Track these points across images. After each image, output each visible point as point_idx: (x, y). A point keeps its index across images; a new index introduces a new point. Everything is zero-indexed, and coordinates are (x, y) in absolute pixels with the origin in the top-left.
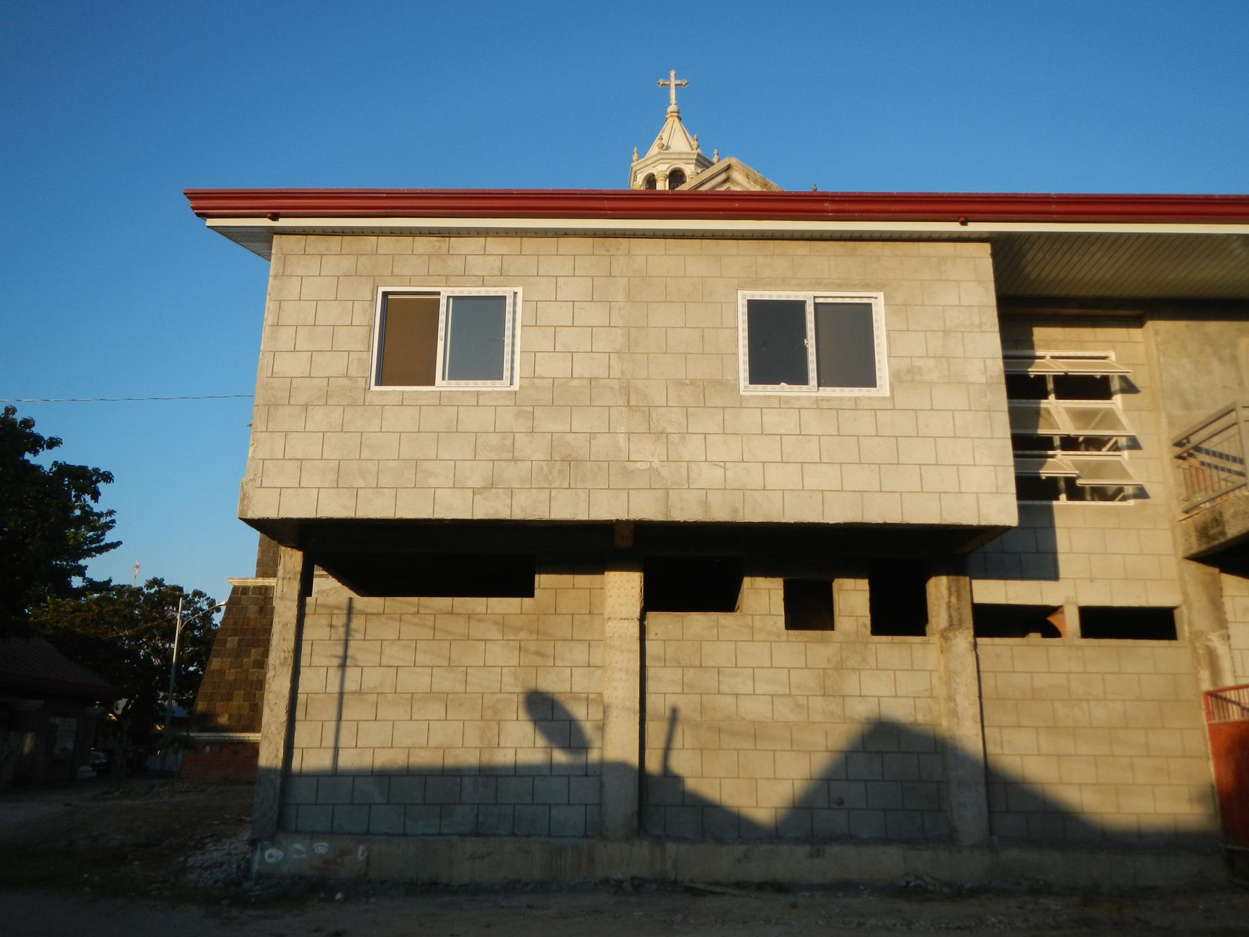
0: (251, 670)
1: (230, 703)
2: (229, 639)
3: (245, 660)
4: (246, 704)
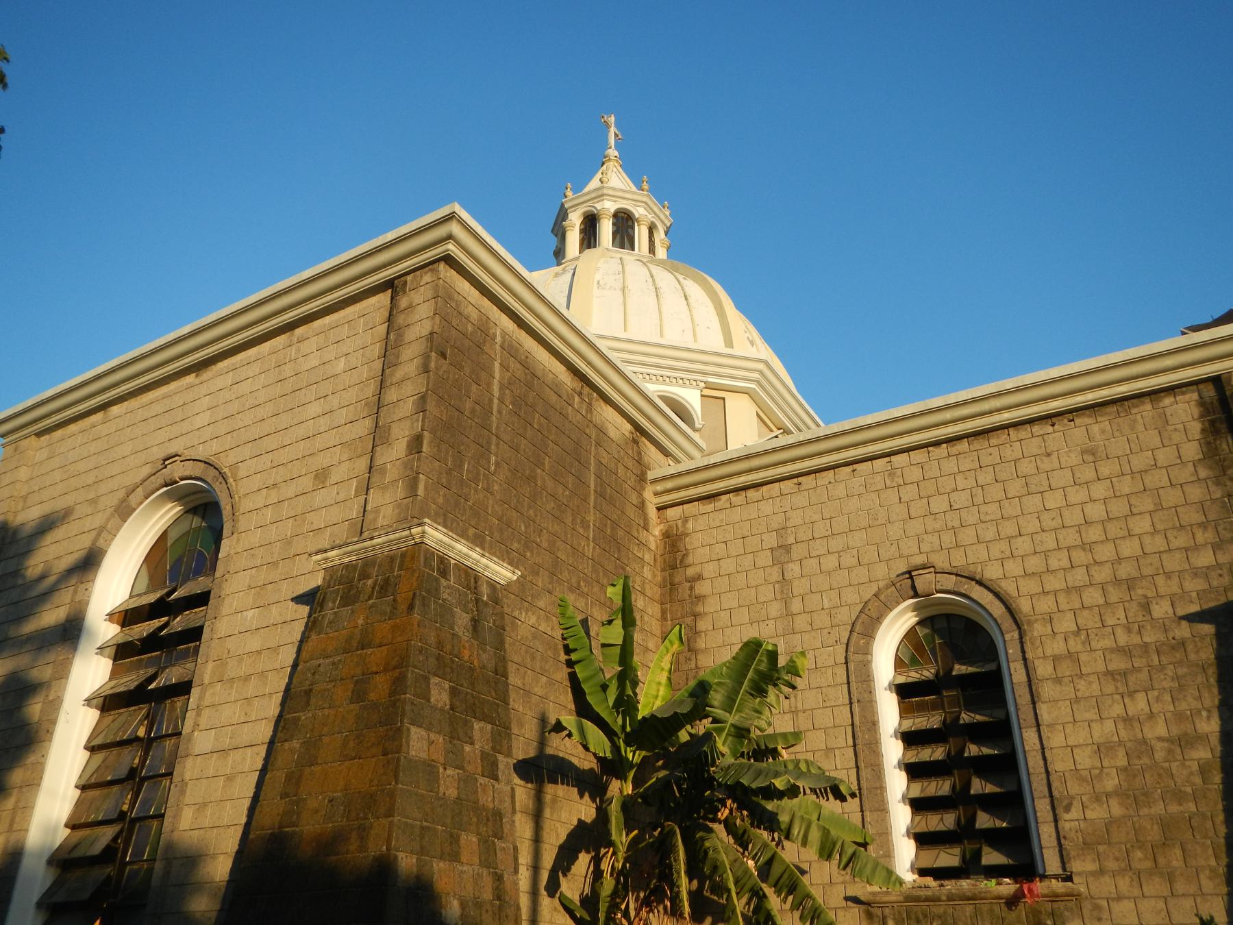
0: (481, 780)
1: (460, 868)
2: (434, 680)
3: (467, 748)
4: (485, 872)
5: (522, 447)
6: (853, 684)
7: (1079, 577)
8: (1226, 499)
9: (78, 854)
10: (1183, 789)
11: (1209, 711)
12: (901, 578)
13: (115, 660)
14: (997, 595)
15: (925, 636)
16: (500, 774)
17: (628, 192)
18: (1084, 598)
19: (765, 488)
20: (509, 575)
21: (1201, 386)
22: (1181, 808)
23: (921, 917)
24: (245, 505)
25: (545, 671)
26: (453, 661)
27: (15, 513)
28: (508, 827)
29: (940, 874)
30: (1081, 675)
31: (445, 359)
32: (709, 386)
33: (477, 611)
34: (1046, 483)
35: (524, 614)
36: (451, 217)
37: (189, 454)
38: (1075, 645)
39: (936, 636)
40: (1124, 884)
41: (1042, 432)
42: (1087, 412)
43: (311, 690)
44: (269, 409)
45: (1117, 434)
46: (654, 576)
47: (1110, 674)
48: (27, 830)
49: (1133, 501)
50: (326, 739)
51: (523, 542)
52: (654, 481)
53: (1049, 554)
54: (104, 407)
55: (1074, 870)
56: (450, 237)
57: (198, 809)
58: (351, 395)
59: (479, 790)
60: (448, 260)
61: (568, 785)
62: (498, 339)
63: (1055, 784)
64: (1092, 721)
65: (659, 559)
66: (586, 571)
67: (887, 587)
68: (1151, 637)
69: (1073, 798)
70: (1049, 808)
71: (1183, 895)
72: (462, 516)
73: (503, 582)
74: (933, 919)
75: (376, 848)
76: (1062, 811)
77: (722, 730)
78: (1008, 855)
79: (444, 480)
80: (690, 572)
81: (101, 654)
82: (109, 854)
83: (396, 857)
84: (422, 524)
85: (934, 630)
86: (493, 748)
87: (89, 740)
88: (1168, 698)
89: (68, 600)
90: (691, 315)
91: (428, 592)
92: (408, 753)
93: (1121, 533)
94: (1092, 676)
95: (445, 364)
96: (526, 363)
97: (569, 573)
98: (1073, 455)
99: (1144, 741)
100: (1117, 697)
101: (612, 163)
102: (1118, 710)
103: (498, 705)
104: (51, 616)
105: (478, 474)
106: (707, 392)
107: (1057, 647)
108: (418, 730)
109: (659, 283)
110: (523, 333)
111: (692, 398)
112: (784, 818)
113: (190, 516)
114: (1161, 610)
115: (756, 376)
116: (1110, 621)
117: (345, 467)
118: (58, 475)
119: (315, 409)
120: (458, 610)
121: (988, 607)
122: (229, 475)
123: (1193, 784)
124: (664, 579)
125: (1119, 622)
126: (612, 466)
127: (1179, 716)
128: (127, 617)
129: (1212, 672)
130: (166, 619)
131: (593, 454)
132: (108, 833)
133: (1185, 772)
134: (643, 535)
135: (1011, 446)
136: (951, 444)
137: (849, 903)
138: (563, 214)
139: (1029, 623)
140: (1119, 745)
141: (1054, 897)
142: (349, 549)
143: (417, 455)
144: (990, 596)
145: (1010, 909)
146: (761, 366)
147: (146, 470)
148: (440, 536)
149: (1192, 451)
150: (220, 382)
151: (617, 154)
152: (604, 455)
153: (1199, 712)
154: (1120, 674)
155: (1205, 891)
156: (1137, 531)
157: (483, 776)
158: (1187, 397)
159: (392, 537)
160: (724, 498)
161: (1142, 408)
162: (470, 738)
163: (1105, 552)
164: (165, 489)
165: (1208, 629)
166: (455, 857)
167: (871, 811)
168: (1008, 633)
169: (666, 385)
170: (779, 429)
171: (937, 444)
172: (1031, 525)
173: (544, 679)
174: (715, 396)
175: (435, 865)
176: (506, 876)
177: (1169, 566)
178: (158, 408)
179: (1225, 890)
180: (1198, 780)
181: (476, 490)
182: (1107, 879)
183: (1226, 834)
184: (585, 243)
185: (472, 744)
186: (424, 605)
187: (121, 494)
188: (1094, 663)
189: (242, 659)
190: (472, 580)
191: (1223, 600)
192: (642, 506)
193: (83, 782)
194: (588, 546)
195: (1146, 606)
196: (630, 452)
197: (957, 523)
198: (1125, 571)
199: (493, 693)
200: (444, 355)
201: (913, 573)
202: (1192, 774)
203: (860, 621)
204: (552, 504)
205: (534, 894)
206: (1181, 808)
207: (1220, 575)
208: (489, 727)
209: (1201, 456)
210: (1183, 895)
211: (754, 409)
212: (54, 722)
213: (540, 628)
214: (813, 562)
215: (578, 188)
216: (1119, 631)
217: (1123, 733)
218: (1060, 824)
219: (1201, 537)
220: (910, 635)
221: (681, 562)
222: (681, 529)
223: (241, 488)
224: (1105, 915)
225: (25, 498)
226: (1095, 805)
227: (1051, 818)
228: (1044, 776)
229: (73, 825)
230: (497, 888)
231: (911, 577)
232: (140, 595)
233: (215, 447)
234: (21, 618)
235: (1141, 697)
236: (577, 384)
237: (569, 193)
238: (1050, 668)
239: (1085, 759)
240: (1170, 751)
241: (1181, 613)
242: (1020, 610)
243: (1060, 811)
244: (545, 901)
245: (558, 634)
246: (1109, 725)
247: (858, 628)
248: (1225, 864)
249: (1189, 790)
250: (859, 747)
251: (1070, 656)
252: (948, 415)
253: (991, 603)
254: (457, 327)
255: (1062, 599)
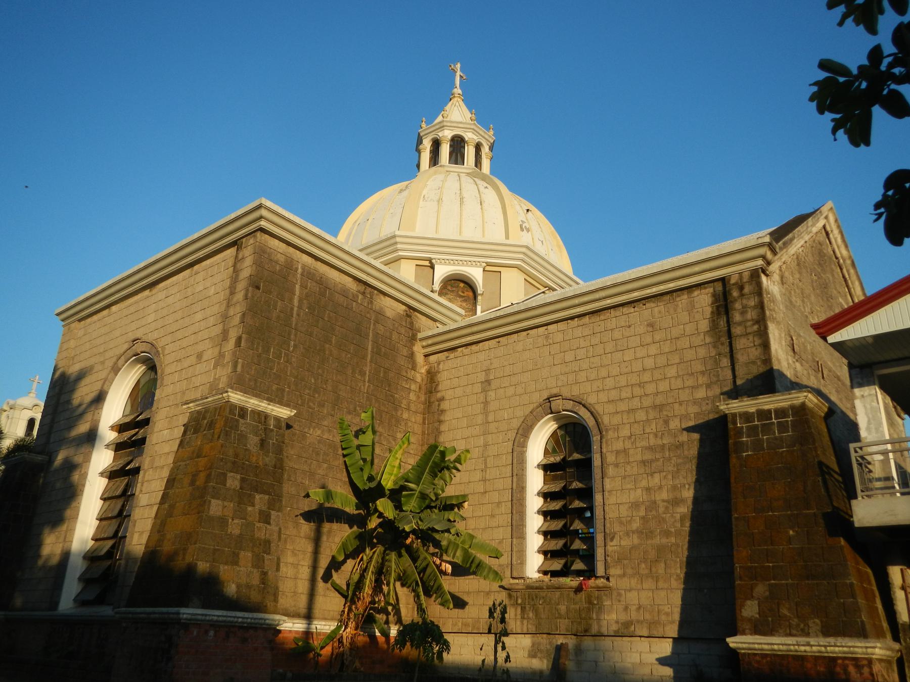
0: (258, 525)
1: (238, 569)
2: (230, 475)
3: (250, 509)
4: (255, 571)
5: (315, 333)
6: (515, 465)
7: (635, 404)
8: (717, 357)
9: (95, 554)
10: (670, 529)
11: (689, 485)
12: (545, 402)
13: (116, 451)
14: (592, 413)
15: (562, 436)
16: (271, 522)
17: (461, 123)
18: (636, 416)
19: (481, 344)
20: (289, 413)
21: (716, 284)
22: (668, 540)
23: (534, 597)
24: (168, 370)
25: (327, 461)
26: (244, 464)
27: (69, 367)
28: (275, 548)
29: (554, 574)
30: (628, 463)
31: (259, 289)
32: (488, 264)
33: (265, 435)
34: (626, 345)
35: (312, 430)
36: (260, 207)
37: (145, 338)
38: (628, 445)
39: (567, 436)
40: (634, 582)
41: (627, 312)
42: (653, 299)
43: (175, 478)
44: (179, 315)
45: (667, 314)
46: (418, 397)
47: (644, 462)
48: (72, 542)
49: (669, 357)
50: (178, 504)
51: (312, 389)
52: (421, 340)
53: (621, 388)
54: (108, 306)
55: (611, 574)
56: (261, 217)
57: (140, 535)
58: (216, 309)
59: (256, 530)
60: (262, 230)
61: (341, 523)
62: (300, 270)
63: (608, 525)
64: (631, 489)
65: (423, 387)
66: (361, 401)
67: (537, 407)
68: (666, 441)
69: (615, 533)
70: (603, 539)
71: (662, 589)
72: (268, 379)
73: (285, 417)
74: (540, 599)
75: (189, 559)
76: (609, 540)
77: (414, 494)
78: (586, 565)
79: (255, 361)
80: (439, 395)
81: (107, 448)
82: (110, 554)
83: (196, 564)
84: (227, 392)
85: (566, 432)
86: (269, 508)
87: (103, 495)
88: (670, 477)
89: (90, 419)
90: (483, 216)
91: (231, 428)
92: (208, 513)
93: (660, 377)
94: (634, 463)
95: (258, 293)
96: (322, 282)
97: (348, 403)
98: (642, 327)
99: (655, 502)
100: (645, 476)
101: (456, 99)
102: (644, 483)
103: (274, 485)
104: (83, 428)
105: (281, 354)
106: (488, 268)
107: (619, 445)
108: (216, 501)
109: (465, 194)
110: (319, 263)
111: (476, 274)
112: (444, 543)
113: (150, 372)
114: (675, 424)
115: (521, 256)
116: (647, 431)
117: (210, 352)
118: (88, 346)
119: (199, 316)
120: (251, 436)
121: (587, 420)
122: (161, 352)
123: (675, 527)
124: (426, 400)
125: (651, 431)
126: (388, 334)
127: (674, 488)
128: (121, 428)
129: (695, 461)
130: (137, 430)
131: (371, 329)
132: (110, 543)
133: (673, 520)
134: (411, 374)
135: (614, 320)
136: (580, 318)
137: (501, 589)
138: (420, 141)
139: (607, 430)
140: (642, 504)
141: (599, 588)
142: (198, 403)
143: (238, 348)
144: (589, 413)
145: (576, 594)
146: (524, 250)
147: (126, 346)
148: (240, 397)
149: (704, 325)
150: (161, 295)
151: (460, 92)
152: (381, 329)
153: (685, 485)
154: (648, 462)
155: (672, 587)
156: (669, 375)
157: (259, 522)
158: (707, 290)
159: (215, 398)
160: (459, 349)
161: (683, 297)
162: (252, 503)
163: (651, 389)
164: (134, 357)
165: (696, 436)
166: (235, 563)
167: (516, 538)
168: (595, 436)
169: (461, 266)
170: (546, 287)
171: (572, 318)
172: (615, 371)
173: (325, 465)
174: (493, 271)
175: (221, 567)
176: (270, 573)
177: (682, 399)
178: (132, 309)
179: (682, 586)
180: (678, 525)
181: (279, 363)
182: (626, 579)
183: (687, 555)
184: (433, 160)
185: (253, 505)
186: (227, 435)
187: (114, 359)
188: (637, 455)
189: (161, 457)
190: (263, 418)
191: (706, 419)
192: (412, 356)
193: (99, 517)
194: (364, 386)
195: (666, 422)
196: (404, 324)
197: (577, 369)
198: (659, 400)
199: (272, 479)
200: (258, 288)
201: (551, 399)
202: (675, 521)
203: (522, 427)
204: (337, 364)
205: (313, 581)
206: (668, 540)
207: (707, 404)
208: (267, 497)
209: (709, 329)
210: (662, 589)
211: (522, 276)
212: (84, 485)
213: (324, 437)
214: (502, 390)
215: (430, 121)
216: (651, 436)
217: (645, 497)
218: (607, 548)
219: (702, 380)
220: (554, 434)
221: (435, 389)
222: (436, 369)
223: (168, 359)
224: (623, 599)
225: (73, 358)
226: (626, 538)
227: (603, 544)
228: (603, 520)
229: (95, 539)
230: (263, 579)
231: (550, 402)
232: (127, 416)
233: (156, 335)
234: (70, 427)
235: (657, 476)
236: (362, 288)
237: (424, 125)
238: (614, 458)
239: (624, 511)
240: (667, 508)
241: (684, 426)
242: (603, 422)
243: (608, 540)
244: (321, 585)
245: (338, 439)
246: (639, 491)
247: (520, 431)
248: (684, 572)
249: (673, 530)
250: (514, 501)
251: (625, 451)
252: (576, 301)
253: (589, 418)
254: (269, 269)
255: (625, 417)
